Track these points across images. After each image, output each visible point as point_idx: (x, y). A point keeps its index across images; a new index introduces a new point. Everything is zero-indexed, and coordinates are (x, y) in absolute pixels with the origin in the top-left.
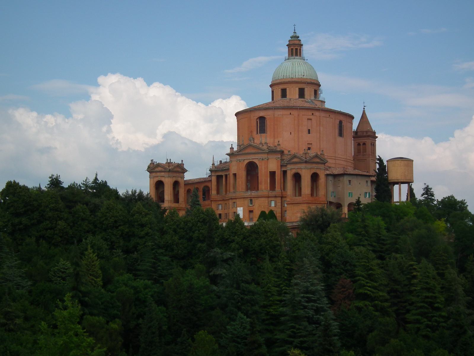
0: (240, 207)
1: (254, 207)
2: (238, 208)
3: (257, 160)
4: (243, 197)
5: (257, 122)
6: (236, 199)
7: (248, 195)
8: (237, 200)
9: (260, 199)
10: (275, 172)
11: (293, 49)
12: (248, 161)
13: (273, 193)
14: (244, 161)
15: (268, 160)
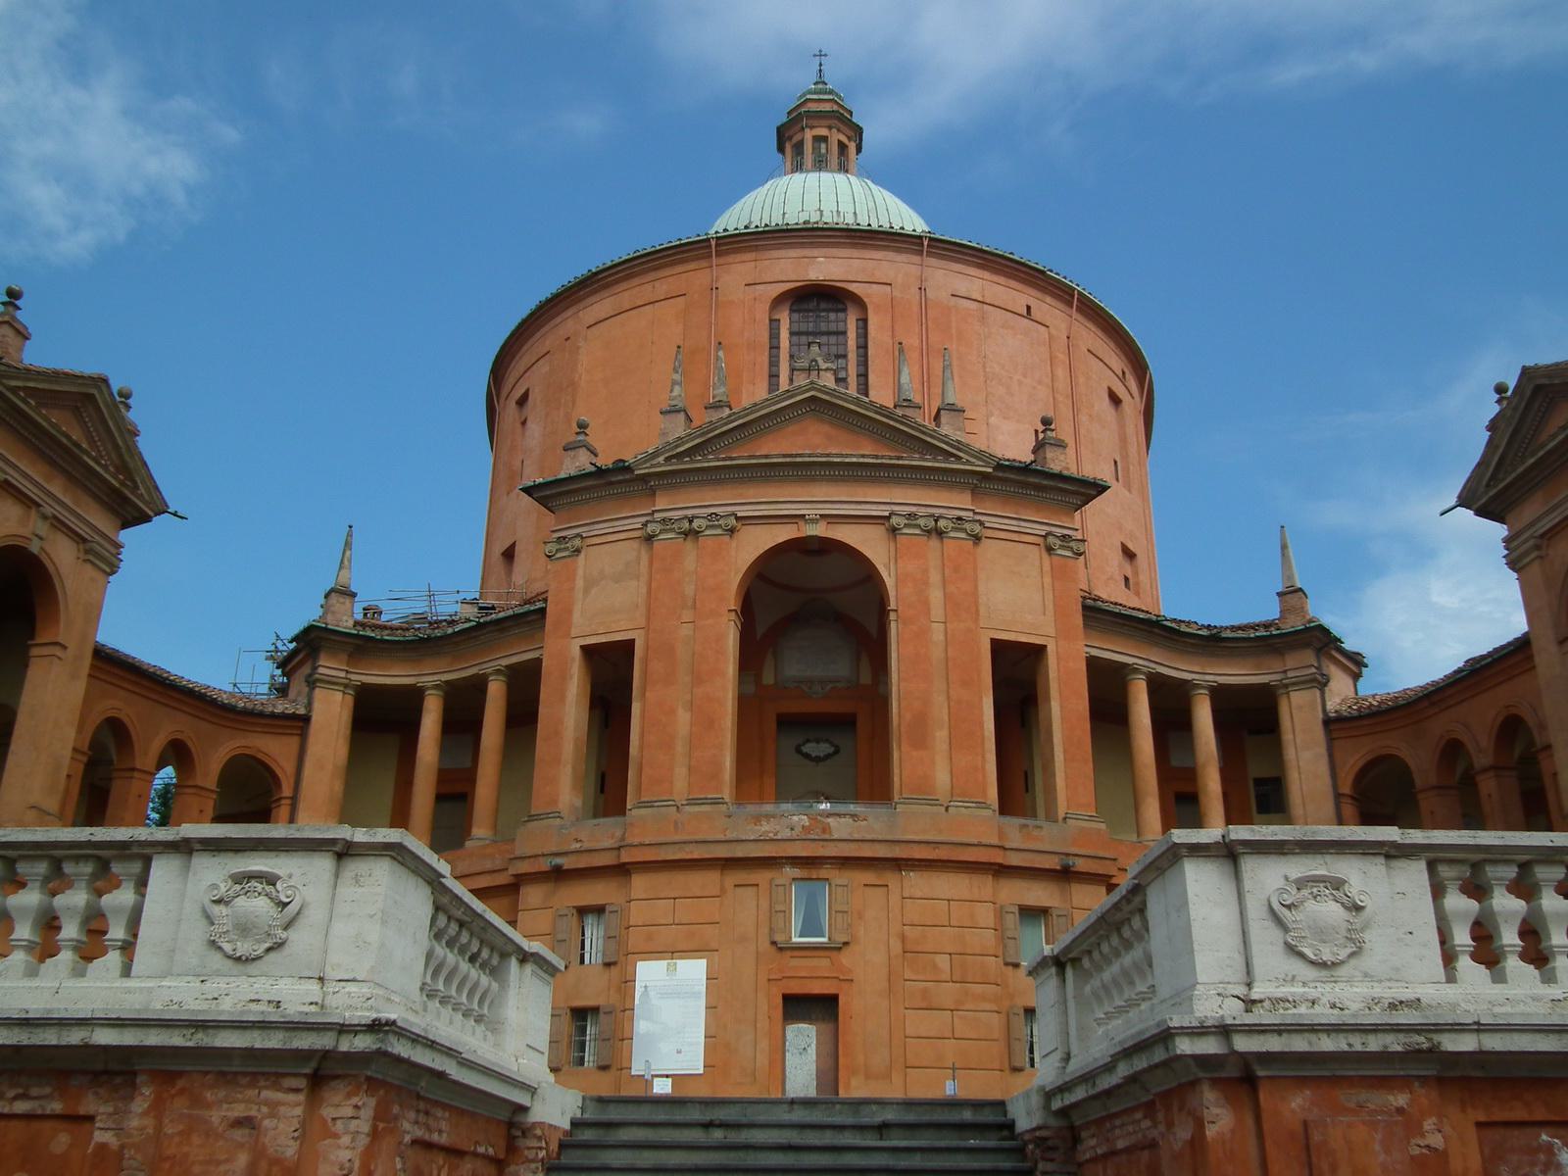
0: (672, 952)
1: (845, 958)
2: (649, 973)
3: (877, 532)
4: (722, 852)
5: (774, 324)
6: (622, 871)
7: (786, 834)
8: (640, 883)
9: (916, 883)
10: (1042, 649)
11: (824, 139)
12: (784, 534)
13: (1018, 838)
14: (732, 531)
15: (977, 539)
